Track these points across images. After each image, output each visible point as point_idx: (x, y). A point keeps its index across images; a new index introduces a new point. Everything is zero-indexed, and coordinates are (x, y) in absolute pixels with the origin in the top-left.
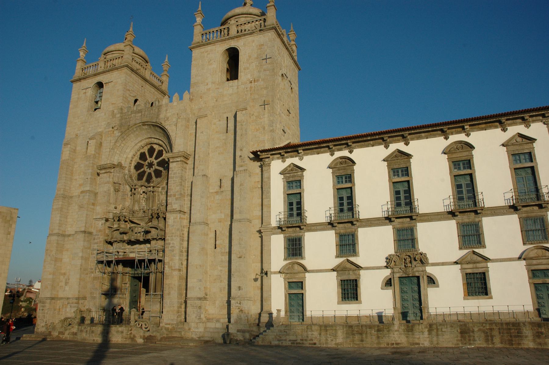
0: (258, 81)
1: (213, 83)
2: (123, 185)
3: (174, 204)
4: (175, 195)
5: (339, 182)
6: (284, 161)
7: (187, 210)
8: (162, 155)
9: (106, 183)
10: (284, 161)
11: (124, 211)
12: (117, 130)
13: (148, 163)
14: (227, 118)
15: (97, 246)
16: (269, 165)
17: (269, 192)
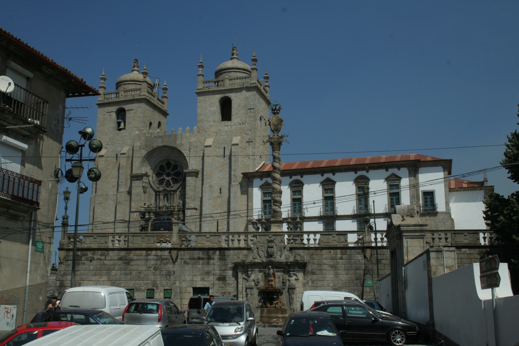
0: (245, 124)
1: (214, 121)
2: (149, 188)
3: (191, 203)
4: (191, 198)
5: (294, 195)
6: (261, 180)
7: (198, 208)
8: (177, 168)
9: (137, 187)
10: (261, 180)
11: (151, 206)
12: (143, 149)
13: (166, 173)
14: (224, 148)
15: (134, 230)
16: (252, 182)
17: (252, 198)
